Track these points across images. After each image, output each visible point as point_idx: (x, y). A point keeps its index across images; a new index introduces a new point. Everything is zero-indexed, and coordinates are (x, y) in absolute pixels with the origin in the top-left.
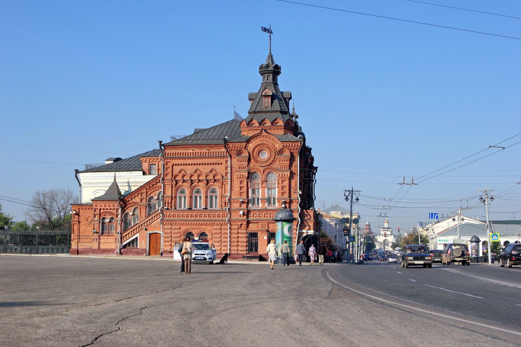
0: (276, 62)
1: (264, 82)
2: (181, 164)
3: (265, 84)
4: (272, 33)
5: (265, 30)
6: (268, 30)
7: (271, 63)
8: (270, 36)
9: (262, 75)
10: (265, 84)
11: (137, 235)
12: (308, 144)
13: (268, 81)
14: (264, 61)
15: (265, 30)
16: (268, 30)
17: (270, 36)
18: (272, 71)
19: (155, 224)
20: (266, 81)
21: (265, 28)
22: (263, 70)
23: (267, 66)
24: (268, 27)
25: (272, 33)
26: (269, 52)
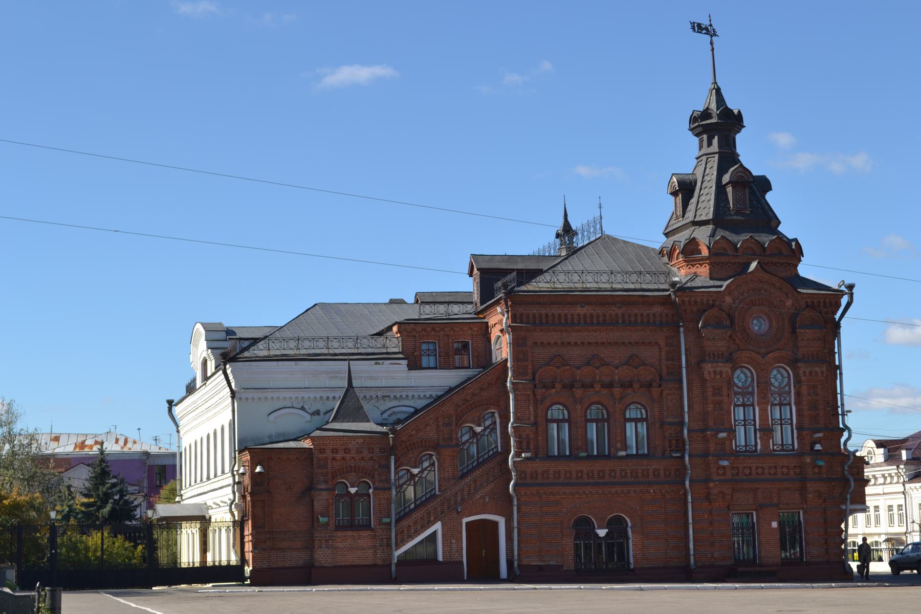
0: (733, 104)
1: (704, 151)
2: (556, 343)
3: (704, 158)
4: (715, 34)
5: (698, 28)
6: (706, 29)
7: (713, 106)
8: (712, 43)
9: (697, 135)
10: (704, 158)
11: (438, 526)
12: (387, 301)
13: (710, 150)
14: (701, 100)
15: (698, 28)
16: (706, 29)
17: (712, 43)
18: (719, 126)
19: (483, 497)
20: (705, 150)
21: (699, 25)
22: (702, 125)
23: (706, 114)
24: (705, 22)
25: (715, 34)
26: (712, 80)
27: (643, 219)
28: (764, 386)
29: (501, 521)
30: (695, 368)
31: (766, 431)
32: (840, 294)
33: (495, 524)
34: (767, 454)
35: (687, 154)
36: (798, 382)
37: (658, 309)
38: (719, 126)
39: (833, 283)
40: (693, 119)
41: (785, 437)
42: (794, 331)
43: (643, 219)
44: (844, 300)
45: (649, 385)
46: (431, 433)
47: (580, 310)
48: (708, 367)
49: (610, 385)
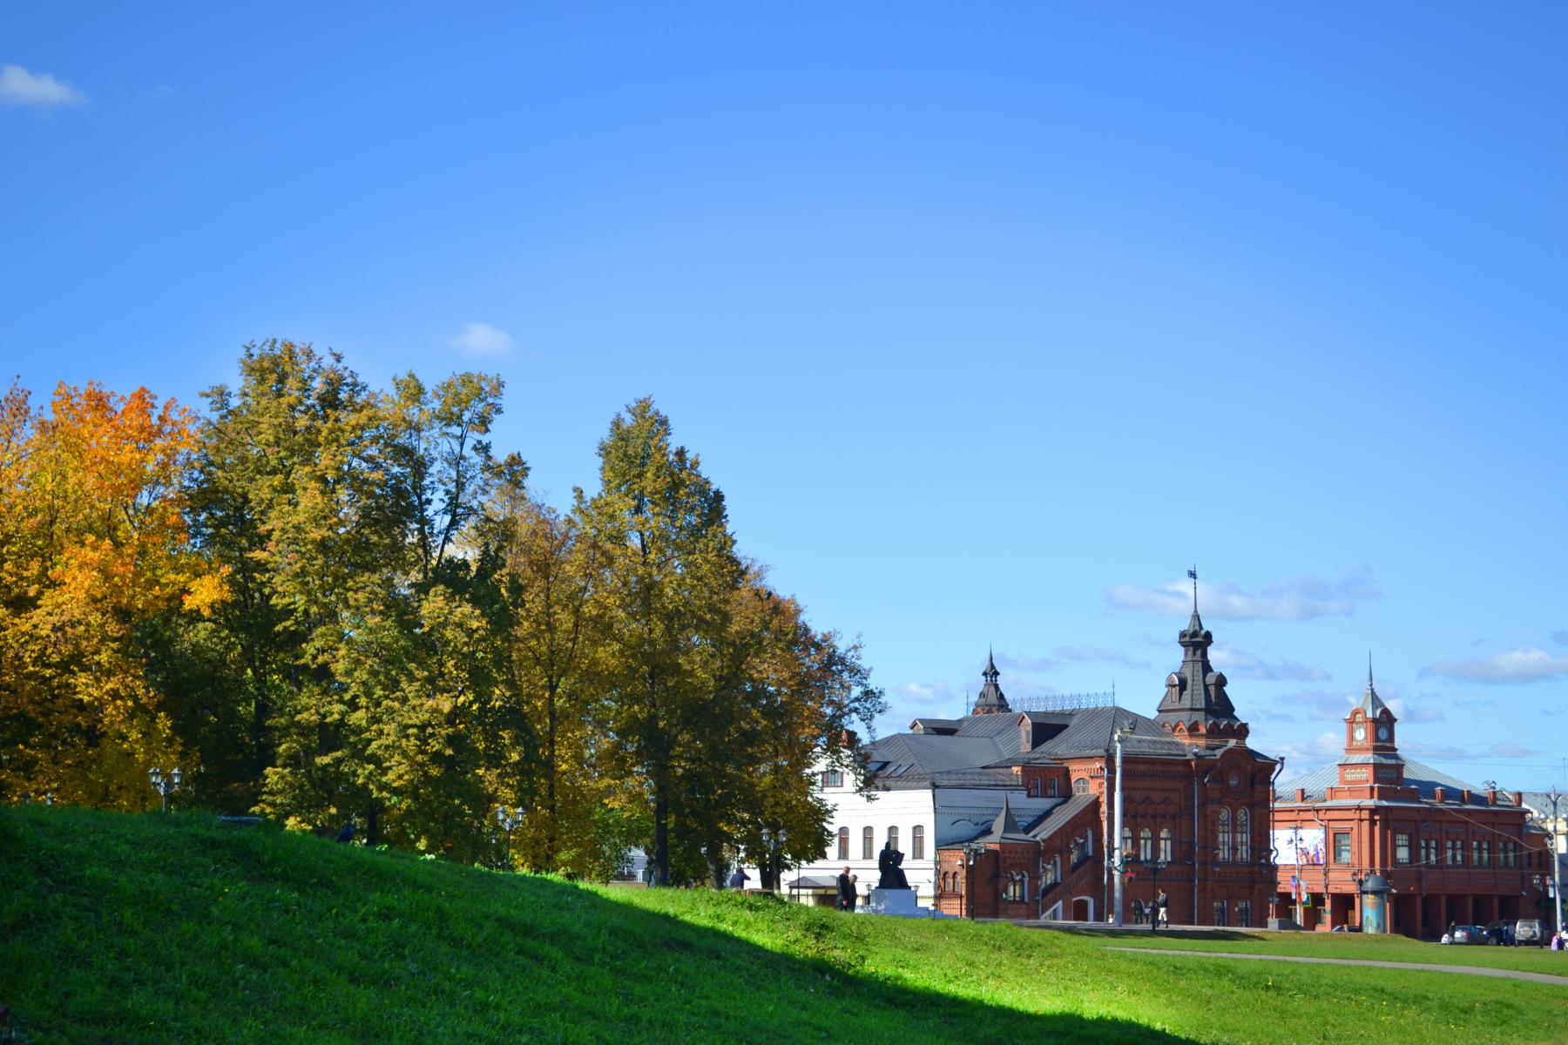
0: (1206, 627)
11: (1060, 903)
18: (1197, 642)
27: (1144, 696)
28: (1234, 819)
29: (1091, 901)
30: (1202, 805)
31: (1235, 849)
32: (1275, 762)
33: (1085, 903)
34: (1235, 864)
35: (1175, 658)
36: (1252, 818)
37: (1181, 768)
38: (1197, 642)
39: (1272, 755)
40: (1183, 635)
41: (1244, 854)
42: (1252, 786)
43: (1144, 696)
44: (1278, 768)
45: (1173, 817)
46: (1058, 843)
47: (1142, 767)
48: (1210, 808)
49: (1154, 817)
